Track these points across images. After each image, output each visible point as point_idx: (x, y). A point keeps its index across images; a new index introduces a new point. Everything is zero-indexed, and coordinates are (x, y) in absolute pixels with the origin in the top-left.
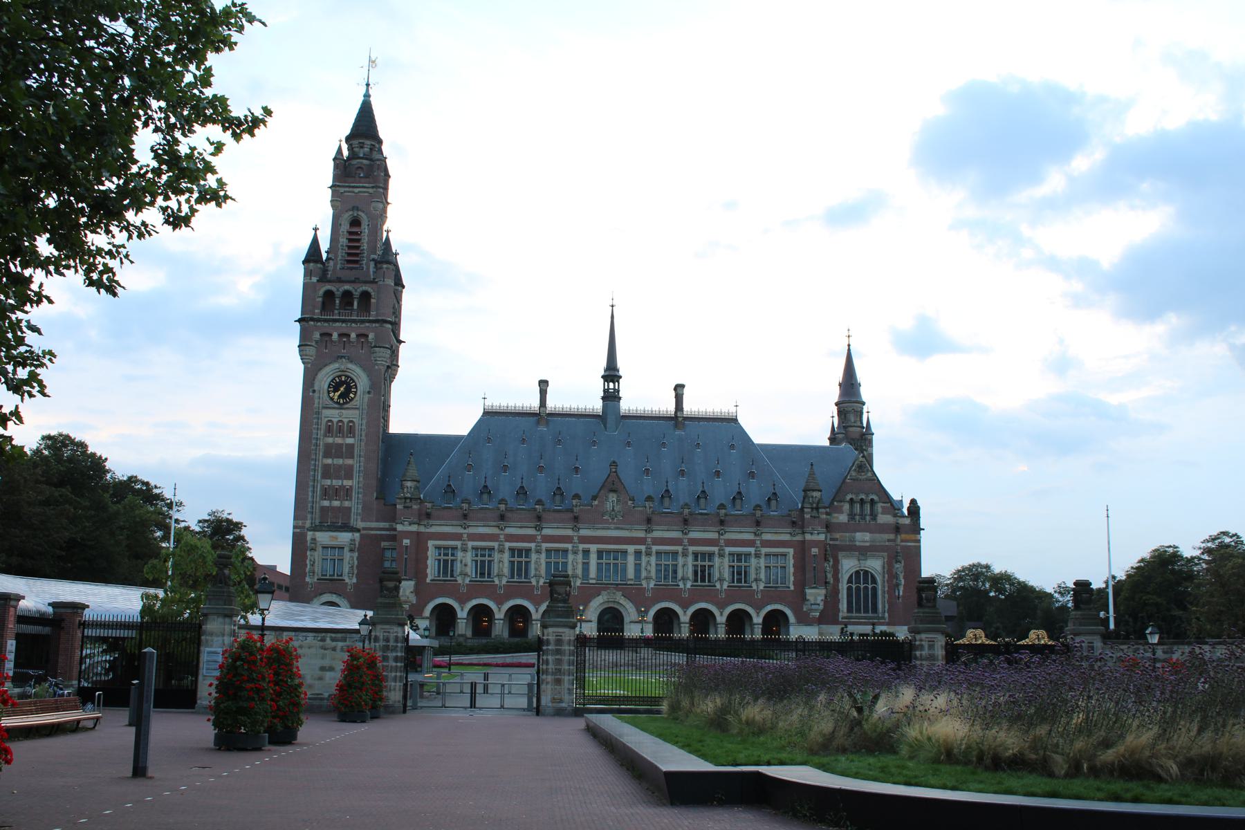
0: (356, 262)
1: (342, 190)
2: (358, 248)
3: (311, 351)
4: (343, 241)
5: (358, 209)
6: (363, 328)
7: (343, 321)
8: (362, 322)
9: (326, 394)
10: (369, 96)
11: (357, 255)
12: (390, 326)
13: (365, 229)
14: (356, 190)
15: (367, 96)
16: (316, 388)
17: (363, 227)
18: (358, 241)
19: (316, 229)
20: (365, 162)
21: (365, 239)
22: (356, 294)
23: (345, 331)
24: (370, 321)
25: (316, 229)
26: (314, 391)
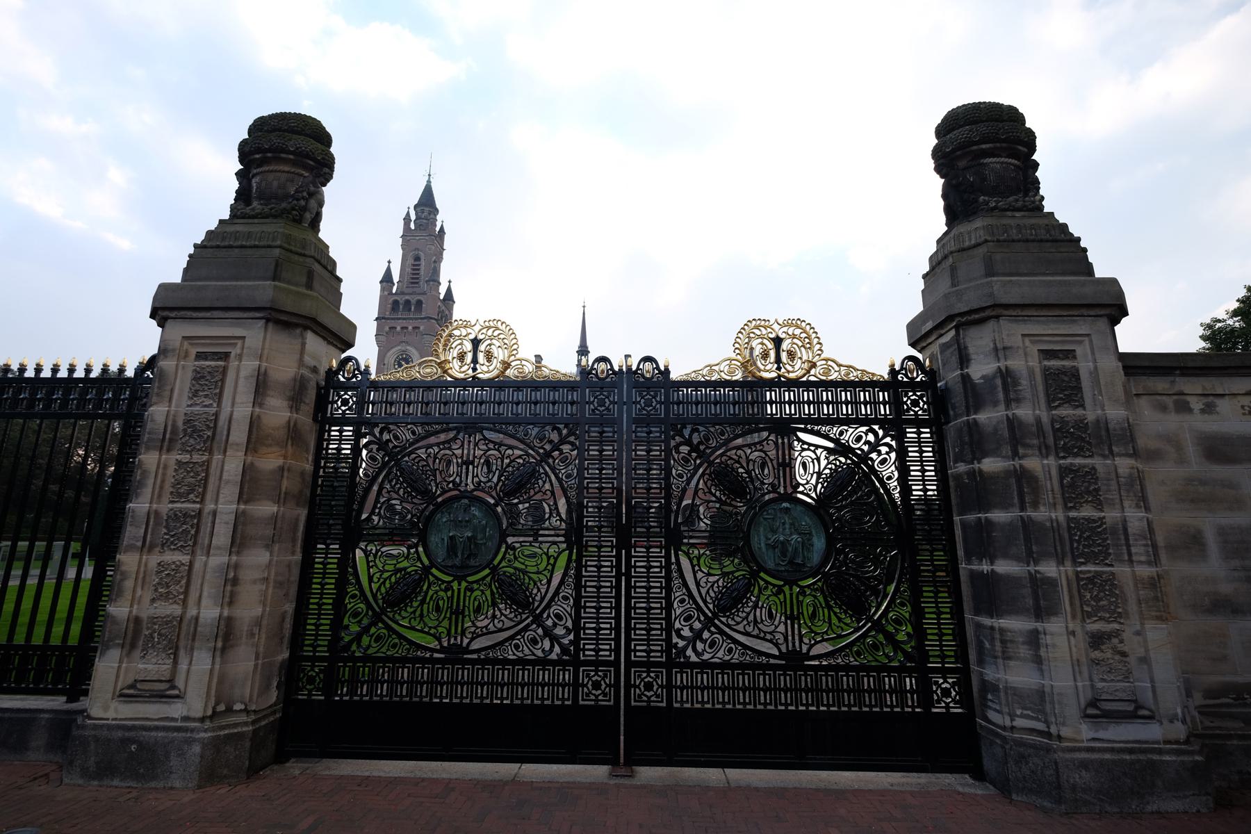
0: (417, 283)
1: (408, 238)
2: (418, 274)
3: (382, 338)
4: (409, 270)
5: (418, 249)
6: (416, 323)
7: (404, 319)
8: (416, 319)
9: (392, 366)
10: (430, 182)
11: (418, 278)
12: (434, 321)
13: (423, 262)
14: (417, 238)
15: (429, 182)
16: (386, 362)
17: (422, 260)
18: (419, 270)
19: (389, 262)
20: (425, 221)
21: (422, 268)
22: (413, 301)
23: (405, 325)
24: (421, 319)
25: (389, 262)
26: (384, 364)
